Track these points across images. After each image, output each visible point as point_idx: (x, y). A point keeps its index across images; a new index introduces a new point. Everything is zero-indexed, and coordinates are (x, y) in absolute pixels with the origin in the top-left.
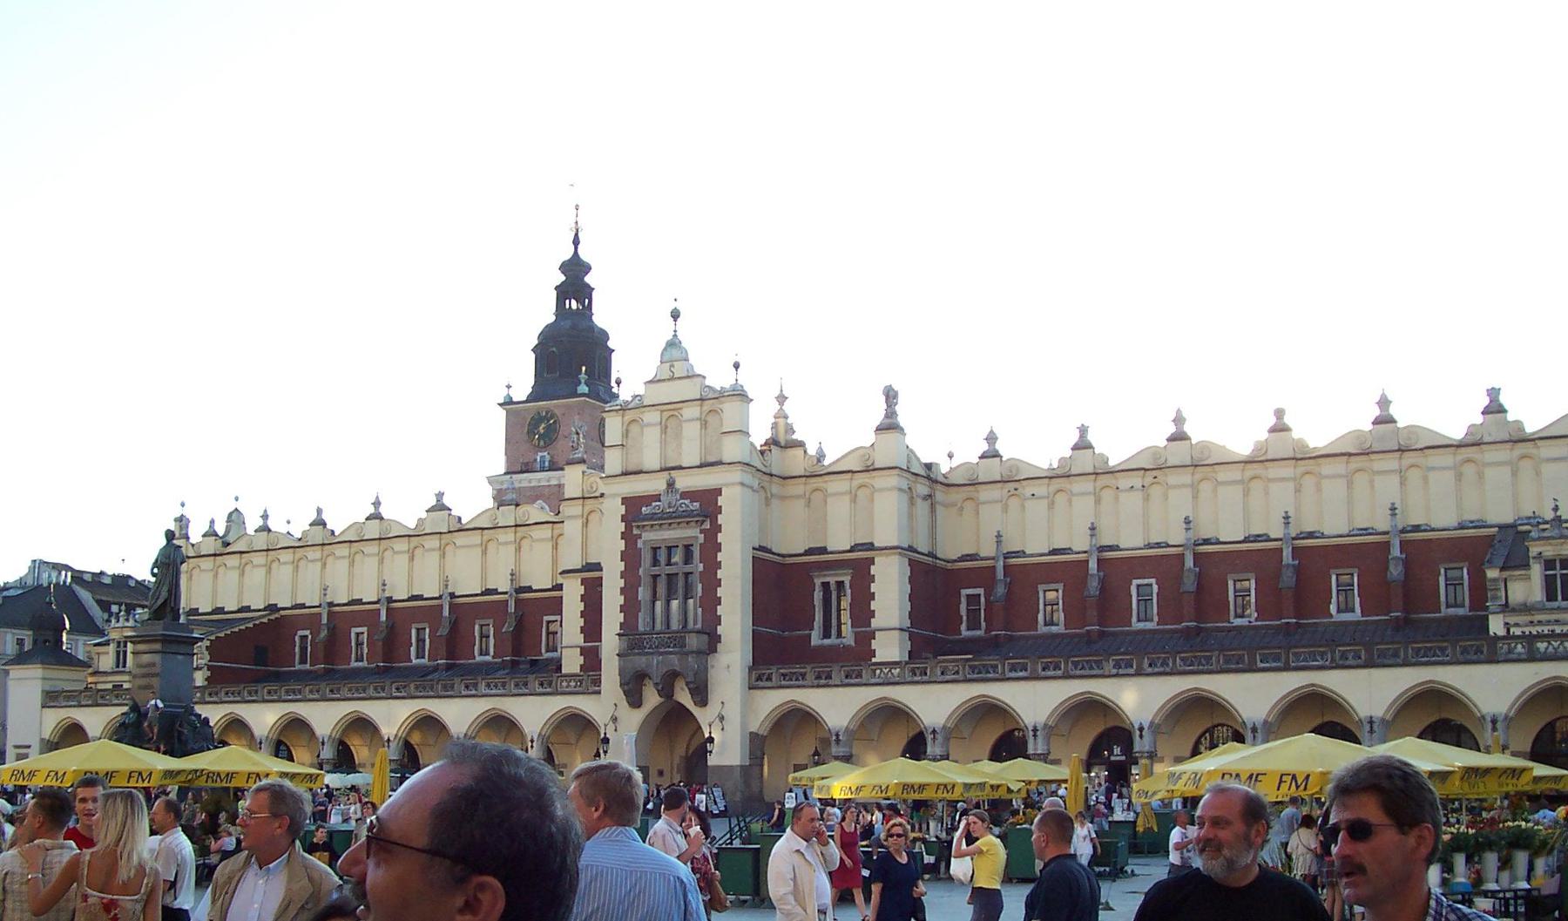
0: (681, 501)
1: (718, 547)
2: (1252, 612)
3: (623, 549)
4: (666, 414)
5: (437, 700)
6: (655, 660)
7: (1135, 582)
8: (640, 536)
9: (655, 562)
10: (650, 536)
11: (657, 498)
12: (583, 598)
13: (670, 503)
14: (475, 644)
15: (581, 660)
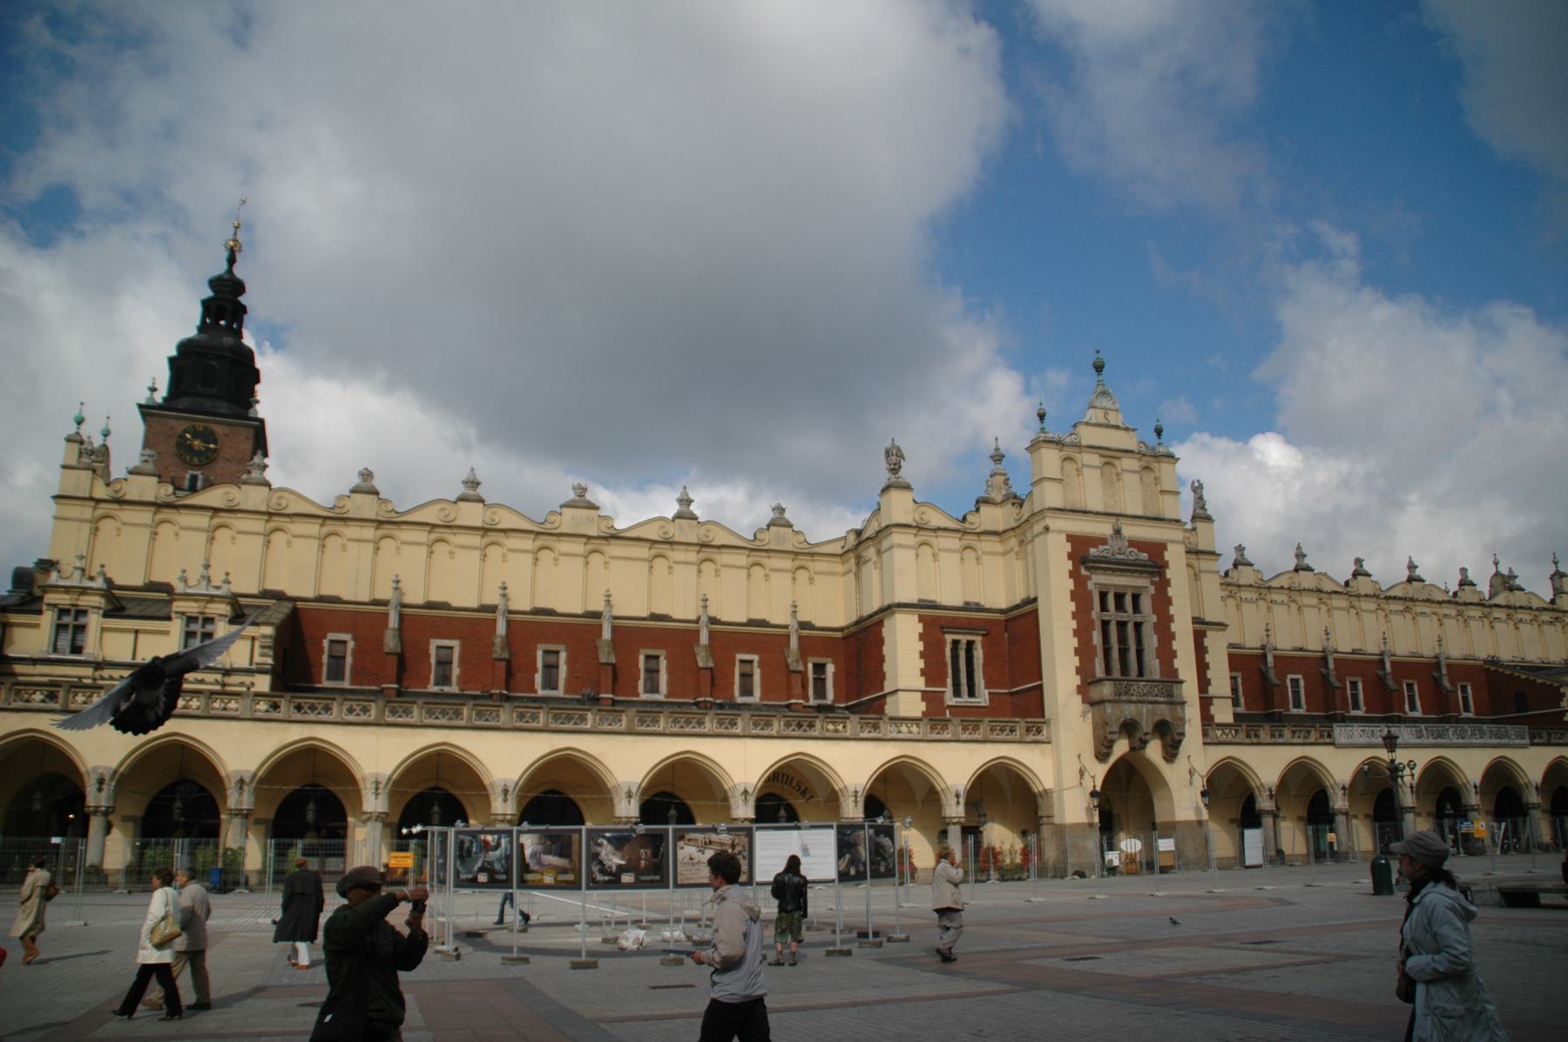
0: (1130, 549)
1: (1169, 602)
2: (1364, 709)
3: (1073, 588)
4: (1104, 460)
5: (821, 743)
6: (1145, 708)
7: (1290, 676)
8: (1089, 578)
9: (1104, 608)
10: (1097, 580)
11: (1103, 541)
12: (922, 637)
13: (1120, 549)
14: (639, 679)
15: (923, 706)
